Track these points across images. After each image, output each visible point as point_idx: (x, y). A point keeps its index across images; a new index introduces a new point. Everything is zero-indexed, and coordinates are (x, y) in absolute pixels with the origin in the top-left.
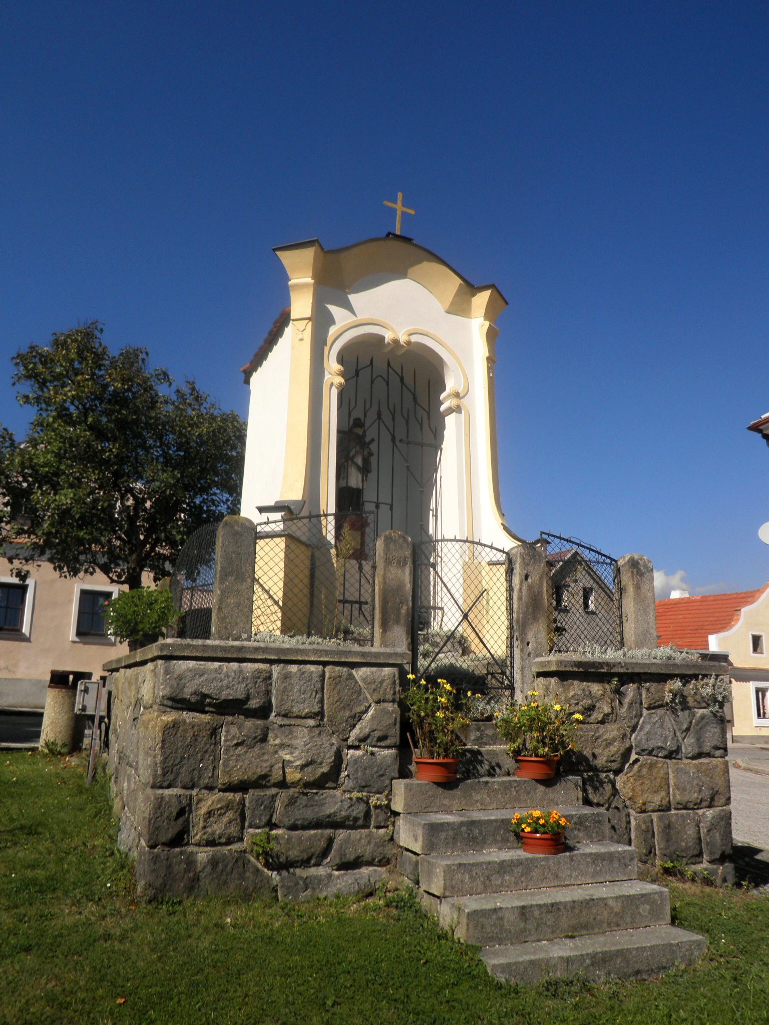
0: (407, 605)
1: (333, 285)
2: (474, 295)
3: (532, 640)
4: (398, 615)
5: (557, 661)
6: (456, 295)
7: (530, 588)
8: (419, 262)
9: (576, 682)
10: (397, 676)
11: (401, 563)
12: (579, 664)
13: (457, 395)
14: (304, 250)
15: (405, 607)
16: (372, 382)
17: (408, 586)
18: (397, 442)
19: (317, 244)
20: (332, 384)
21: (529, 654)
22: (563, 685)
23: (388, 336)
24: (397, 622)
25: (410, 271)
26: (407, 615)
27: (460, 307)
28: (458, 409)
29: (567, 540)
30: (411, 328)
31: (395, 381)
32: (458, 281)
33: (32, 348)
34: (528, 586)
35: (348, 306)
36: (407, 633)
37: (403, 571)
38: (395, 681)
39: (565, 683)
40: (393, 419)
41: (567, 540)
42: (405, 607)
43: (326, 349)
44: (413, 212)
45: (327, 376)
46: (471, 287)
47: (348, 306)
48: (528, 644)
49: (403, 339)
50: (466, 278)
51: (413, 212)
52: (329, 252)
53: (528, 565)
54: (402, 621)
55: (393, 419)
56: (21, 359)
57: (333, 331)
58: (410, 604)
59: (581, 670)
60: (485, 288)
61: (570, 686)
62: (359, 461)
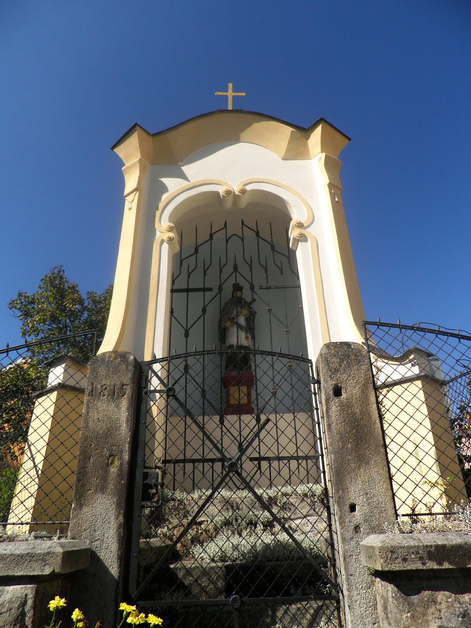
0: (121, 458)
1: (164, 159)
2: (308, 138)
3: (359, 502)
4: (105, 478)
5: (381, 549)
6: (290, 142)
7: (345, 408)
8: (249, 125)
9: (441, 596)
10: (30, 602)
11: (115, 394)
12: (439, 552)
13: (300, 225)
14: (131, 138)
15: (117, 463)
16: (227, 241)
17: (124, 430)
18: (256, 289)
19: (137, 128)
20: (163, 241)
21: (357, 528)
22: (411, 604)
23: (221, 190)
24: (103, 489)
25: (243, 135)
26: (120, 475)
27: (296, 151)
28: (303, 238)
29: (412, 328)
30: (246, 179)
31: (249, 235)
32: (288, 130)
33: (20, 295)
34: (341, 405)
35: (183, 176)
36: (118, 506)
37: (118, 406)
38: (23, 614)
39: (415, 599)
40: (251, 270)
41: (412, 328)
42: (117, 463)
43: (158, 213)
44: (244, 94)
45: (158, 234)
46: (304, 130)
47: (183, 176)
48: (353, 508)
49: (236, 189)
50: (296, 124)
51: (244, 94)
52: (154, 135)
53: (337, 371)
54: (111, 486)
55: (251, 270)
56: (12, 305)
57: (165, 197)
58: (126, 457)
59: (446, 565)
60: (315, 125)
61: (427, 606)
62: (242, 321)
